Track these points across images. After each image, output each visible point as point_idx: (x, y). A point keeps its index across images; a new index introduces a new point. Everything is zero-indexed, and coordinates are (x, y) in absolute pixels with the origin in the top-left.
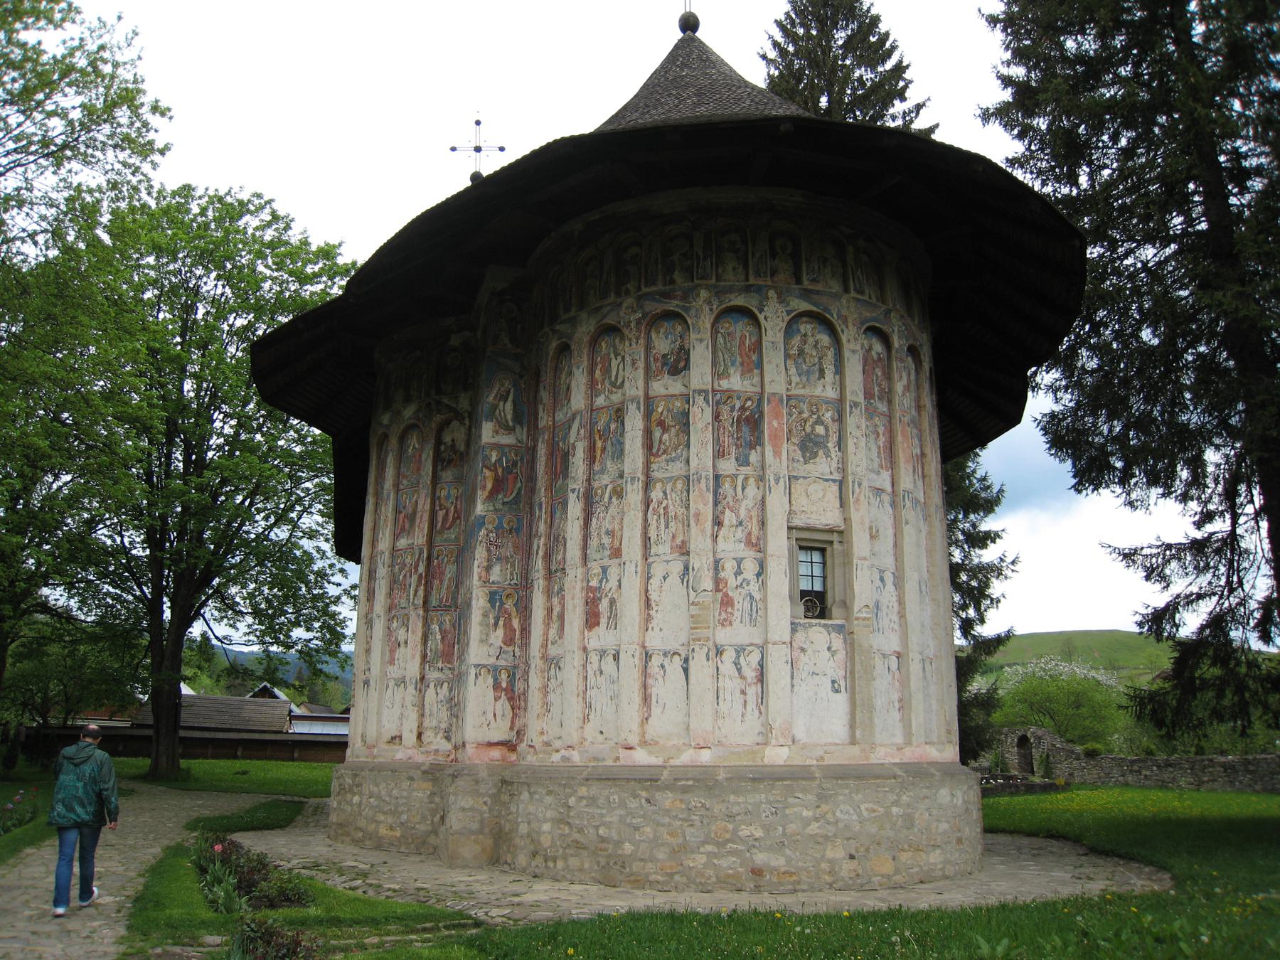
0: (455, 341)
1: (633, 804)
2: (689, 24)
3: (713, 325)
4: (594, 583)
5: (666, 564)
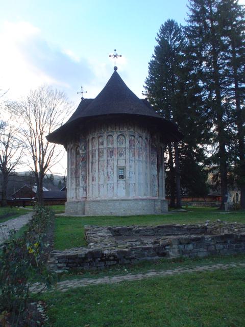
2: (116, 68)
3: (107, 138)
5: (101, 172)
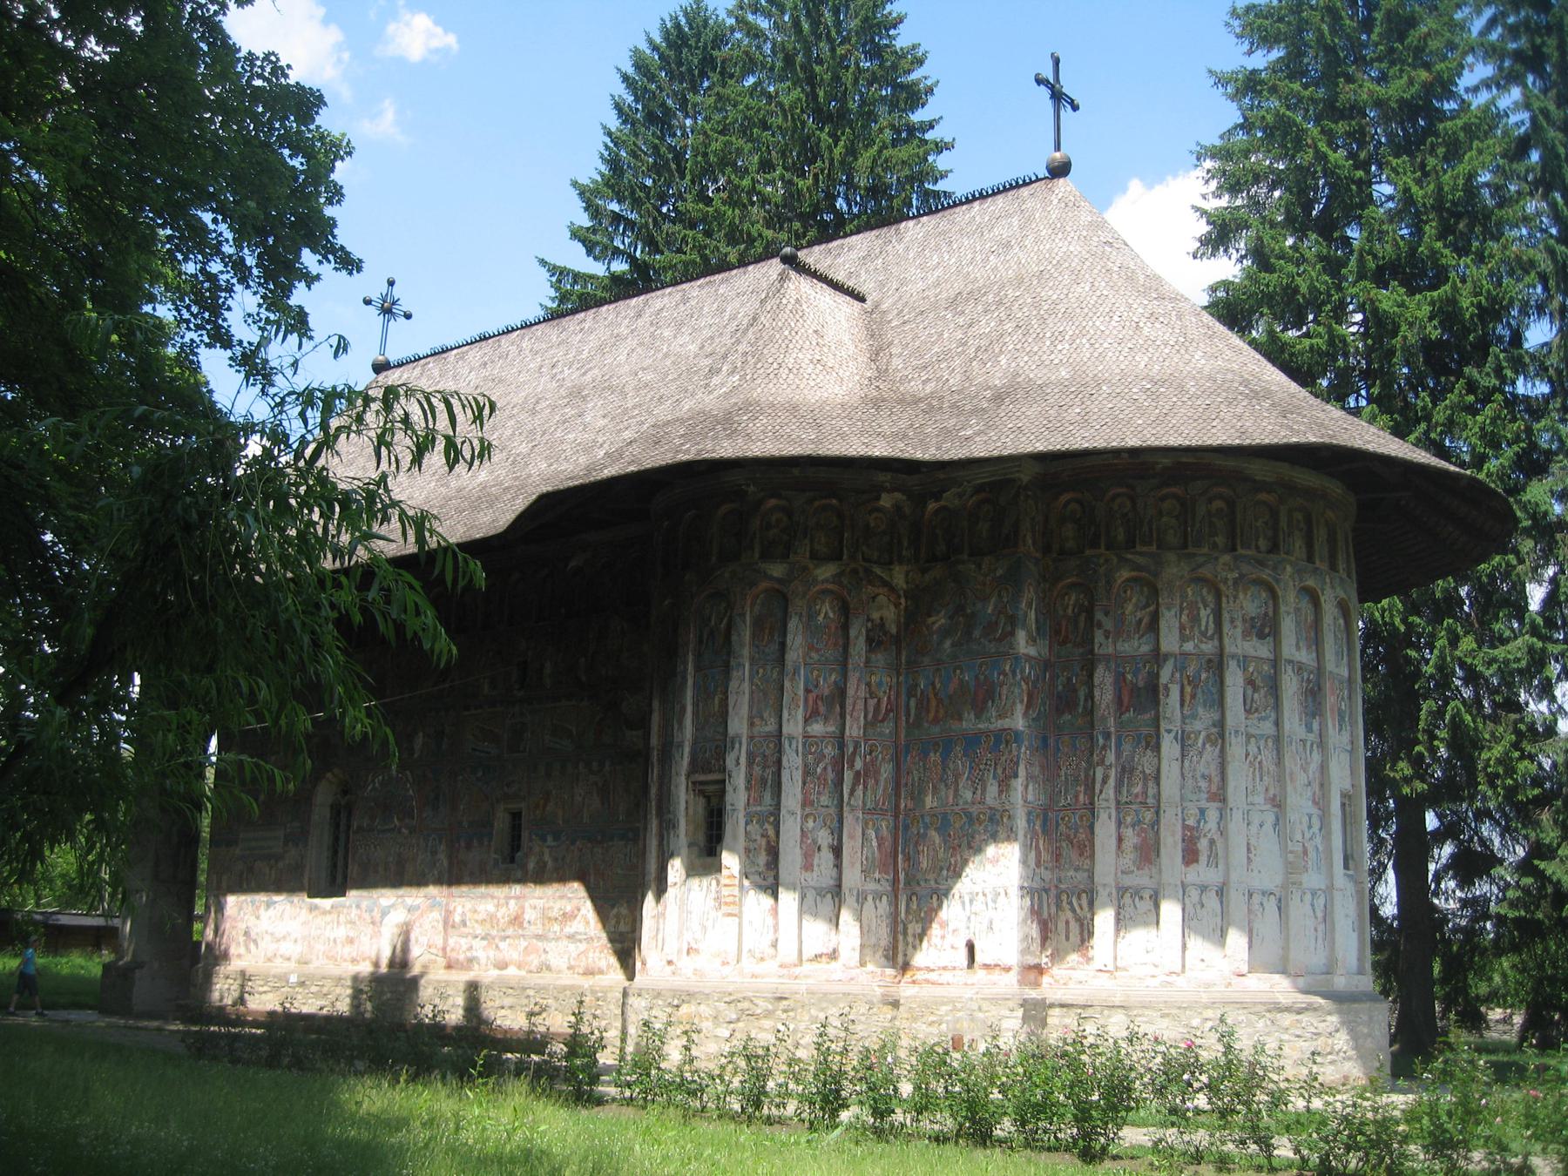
0: (886, 501)
1: (1261, 1024)
4: (1191, 822)
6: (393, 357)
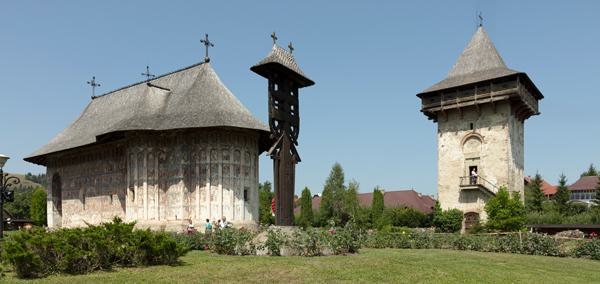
6: (96, 95)
